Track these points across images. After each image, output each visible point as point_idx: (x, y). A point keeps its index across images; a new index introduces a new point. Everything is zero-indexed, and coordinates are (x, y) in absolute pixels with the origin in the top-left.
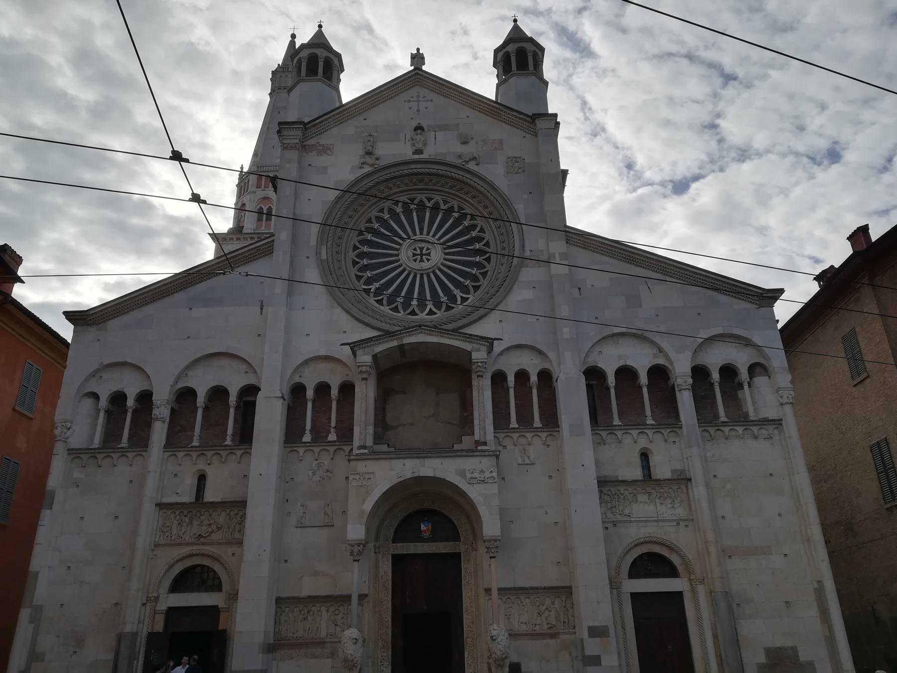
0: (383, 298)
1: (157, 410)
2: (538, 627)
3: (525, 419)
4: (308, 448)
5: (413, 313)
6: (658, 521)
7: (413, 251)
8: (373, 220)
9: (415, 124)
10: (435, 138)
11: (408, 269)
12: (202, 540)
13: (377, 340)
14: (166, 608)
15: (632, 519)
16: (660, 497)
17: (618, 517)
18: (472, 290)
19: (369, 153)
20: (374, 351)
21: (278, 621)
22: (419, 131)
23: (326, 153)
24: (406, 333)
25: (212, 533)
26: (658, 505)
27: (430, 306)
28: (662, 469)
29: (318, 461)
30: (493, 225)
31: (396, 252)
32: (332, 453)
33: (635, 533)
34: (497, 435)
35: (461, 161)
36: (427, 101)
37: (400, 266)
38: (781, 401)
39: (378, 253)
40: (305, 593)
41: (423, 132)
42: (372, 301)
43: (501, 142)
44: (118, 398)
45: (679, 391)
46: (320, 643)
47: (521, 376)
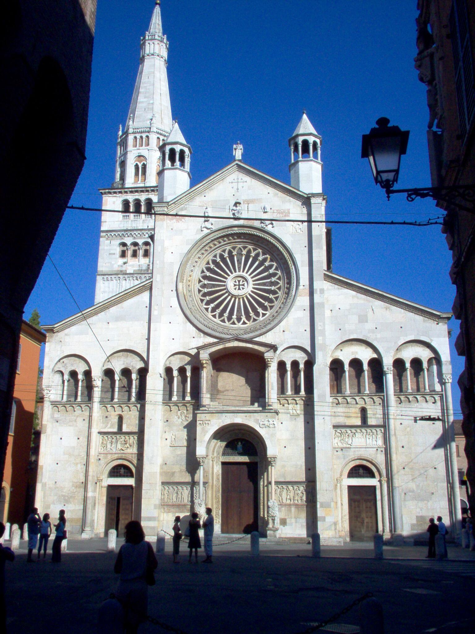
1: (94, 382)
5: (234, 323)
6: (366, 448)
8: (211, 262)
12: (122, 452)
14: (107, 485)
15: (351, 447)
17: (345, 445)
21: (163, 493)
22: (238, 205)
26: (367, 439)
27: (244, 318)
29: (180, 411)
33: (352, 454)
36: (243, 182)
42: (210, 315)
44: (74, 374)
47: (295, 364)
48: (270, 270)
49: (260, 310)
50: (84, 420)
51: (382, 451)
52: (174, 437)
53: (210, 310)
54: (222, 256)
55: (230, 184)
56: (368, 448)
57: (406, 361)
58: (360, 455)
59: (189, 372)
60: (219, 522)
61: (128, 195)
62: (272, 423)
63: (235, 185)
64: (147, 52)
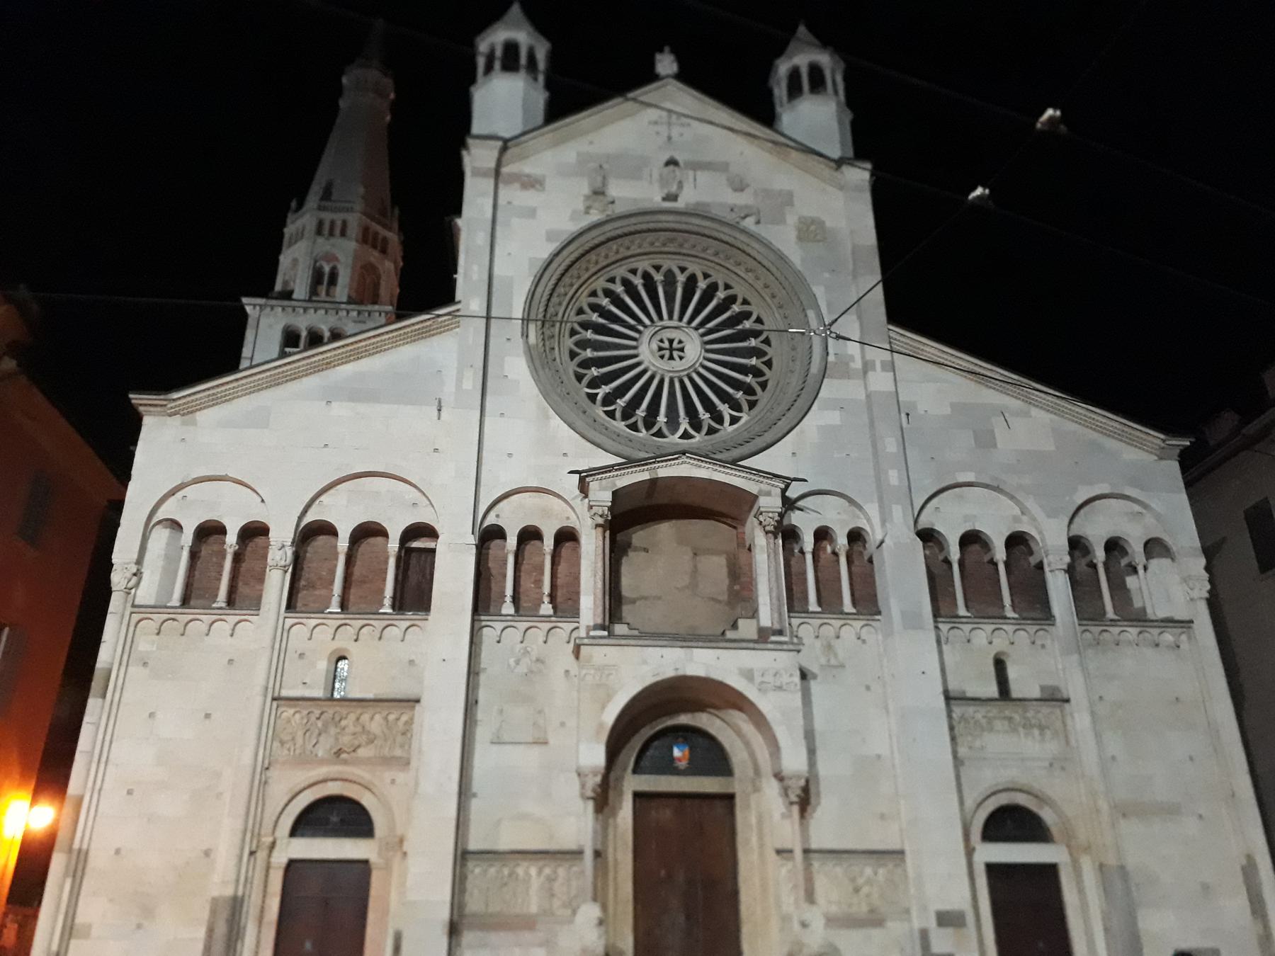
0: (615, 409)
3: (829, 601)
4: (509, 623)
5: (659, 434)
7: (659, 343)
8: (600, 293)
9: (666, 157)
13: (620, 469)
14: (284, 861)
18: (745, 406)
19: (598, 193)
20: (615, 485)
22: (671, 167)
23: (533, 186)
24: (662, 461)
25: (359, 746)
27: (684, 425)
31: (633, 343)
35: (734, 215)
37: (638, 364)
39: (607, 343)
40: (504, 844)
42: (599, 411)
44: (210, 531)
45: (1051, 571)
47: (822, 535)
48: (745, 322)
49: (724, 409)
62: (791, 680)
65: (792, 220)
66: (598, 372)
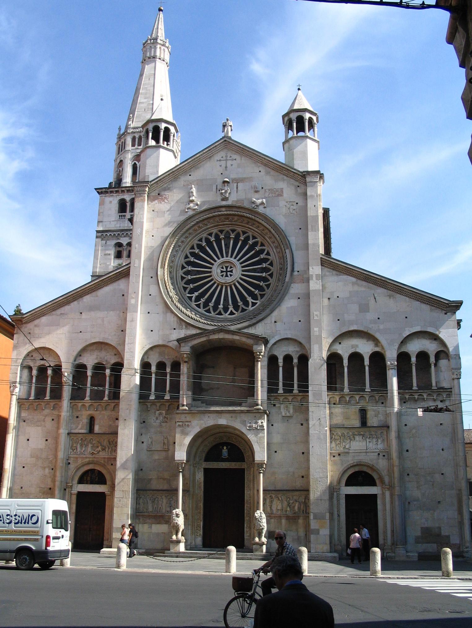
2: (288, 512)
5: (220, 314)
6: (366, 452)
8: (195, 247)
10: (237, 188)
11: (217, 282)
14: (77, 492)
16: (370, 438)
18: (259, 297)
21: (138, 502)
26: (367, 442)
27: (231, 308)
28: (372, 421)
30: (275, 250)
32: (167, 406)
34: (270, 397)
36: (232, 160)
37: (212, 280)
38: (453, 377)
41: (229, 184)
43: (282, 189)
44: (42, 370)
46: (162, 516)
47: (288, 358)
48: (261, 255)
49: (250, 300)
50: (53, 420)
51: (384, 456)
52: (150, 441)
53: (193, 299)
54: (208, 241)
55: (218, 162)
56: (368, 452)
57: (411, 355)
58: (358, 461)
59: (168, 367)
60: (200, 534)
61: (125, 194)
63: (223, 163)
64: (148, 55)
65: (282, 203)
66: (193, 286)
